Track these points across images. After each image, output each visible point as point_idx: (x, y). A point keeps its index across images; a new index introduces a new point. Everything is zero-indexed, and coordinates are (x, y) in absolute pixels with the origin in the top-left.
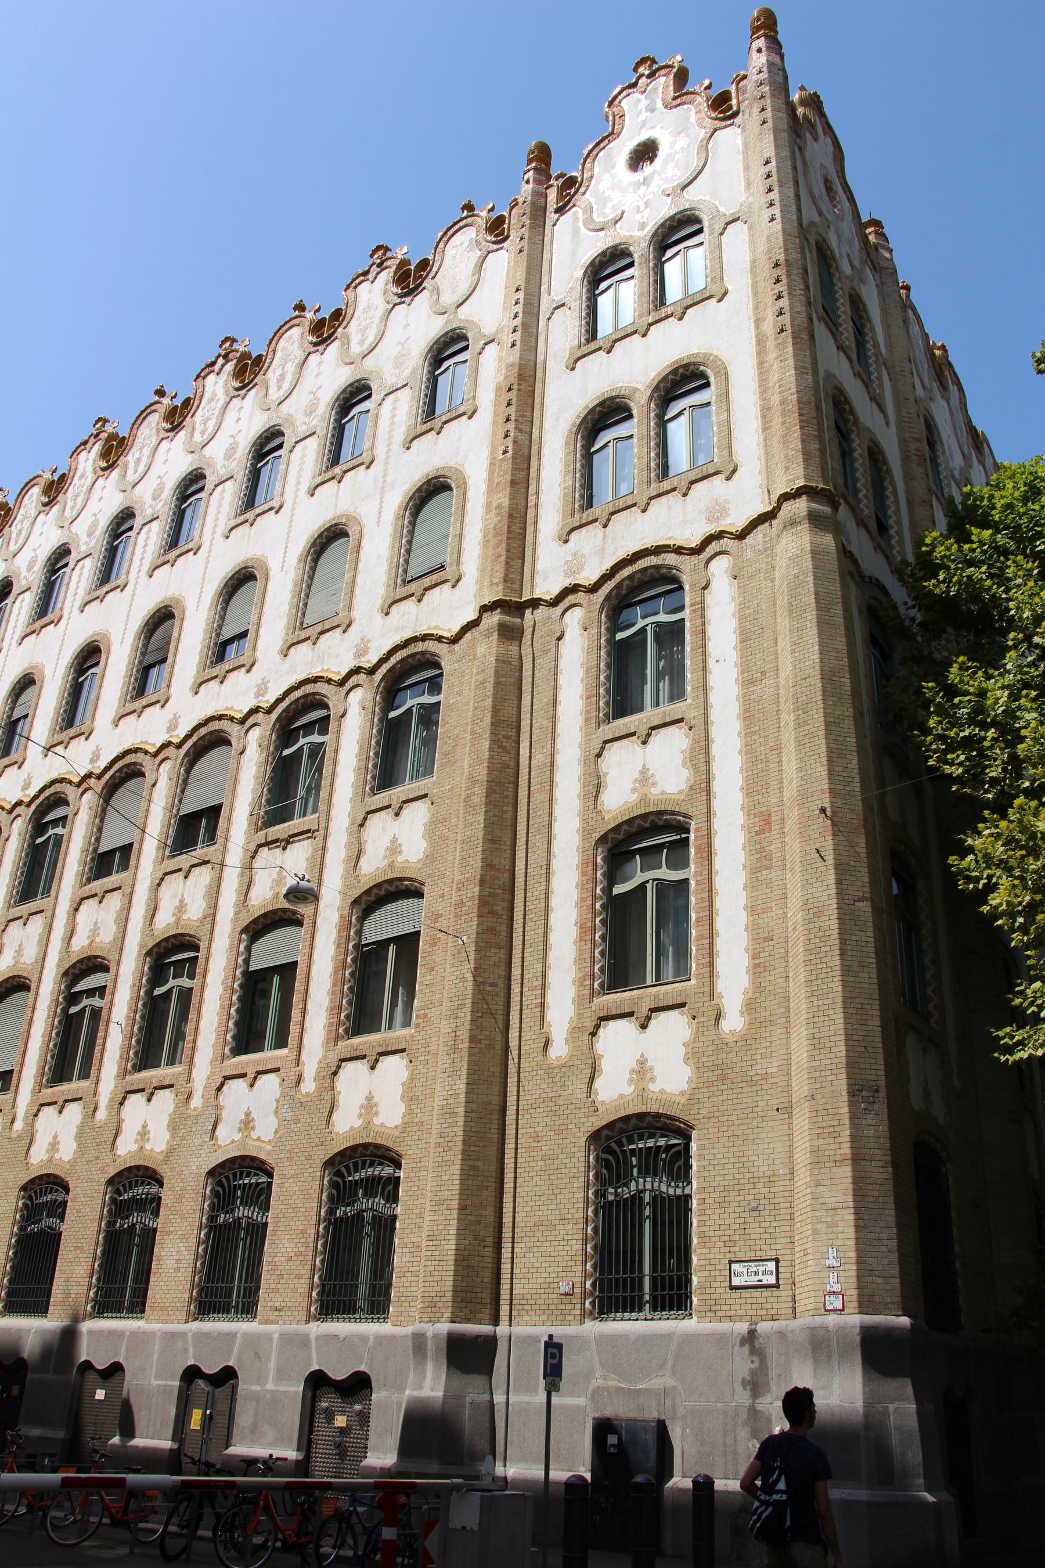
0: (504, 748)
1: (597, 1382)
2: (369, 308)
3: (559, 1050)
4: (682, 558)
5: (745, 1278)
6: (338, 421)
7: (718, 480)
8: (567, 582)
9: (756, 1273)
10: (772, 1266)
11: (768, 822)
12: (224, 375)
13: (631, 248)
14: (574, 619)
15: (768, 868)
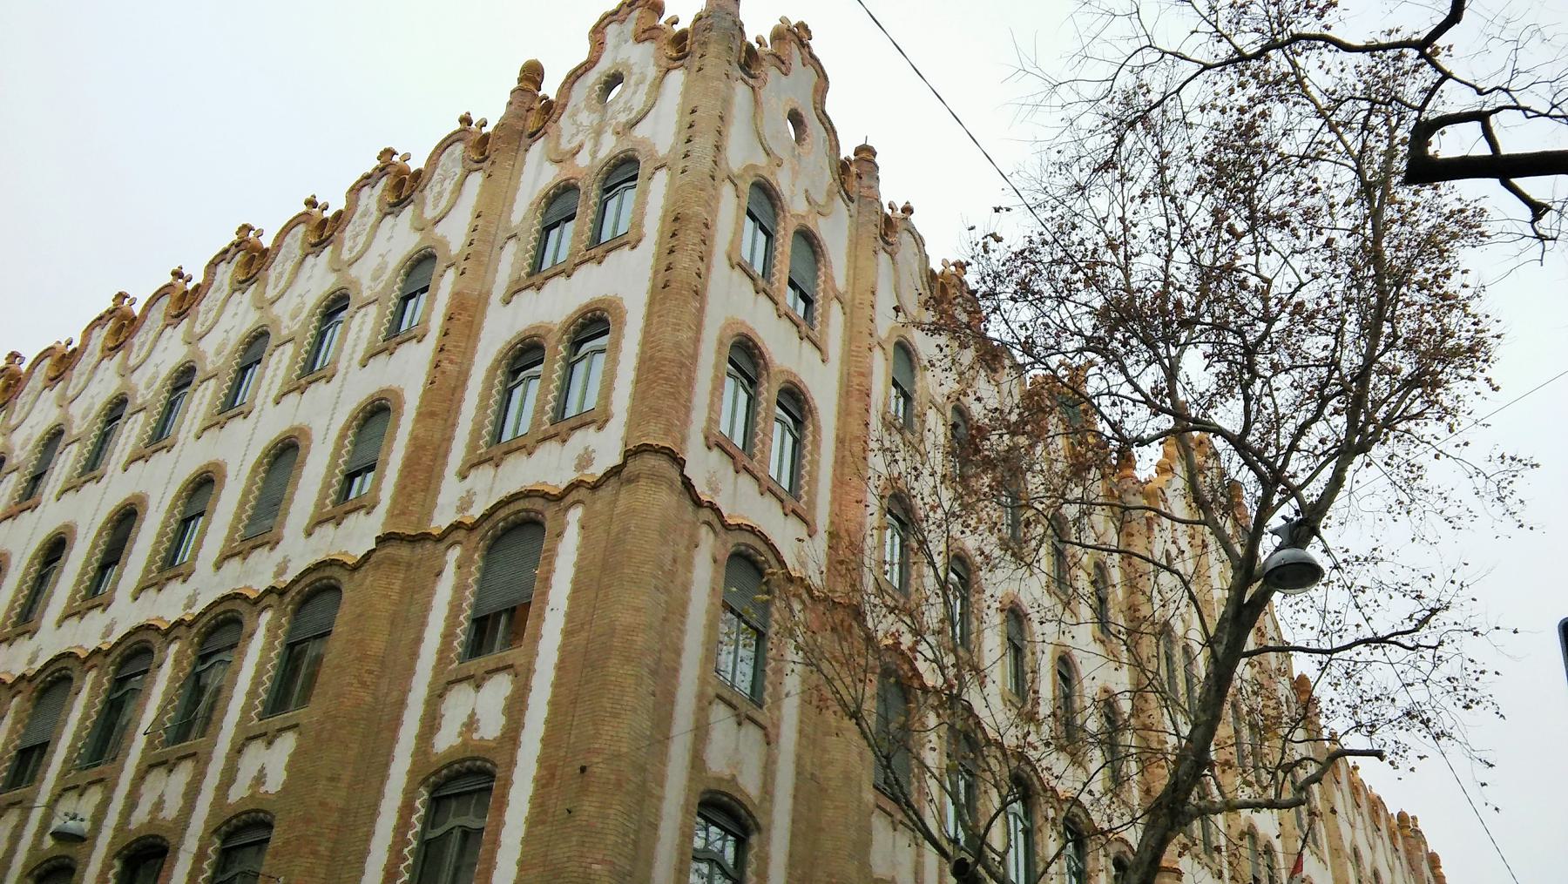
0: (364, 684)
2: (364, 215)
7: (592, 429)
8: (458, 518)
11: (553, 776)
12: (233, 265)
14: (454, 554)
15: (543, 822)
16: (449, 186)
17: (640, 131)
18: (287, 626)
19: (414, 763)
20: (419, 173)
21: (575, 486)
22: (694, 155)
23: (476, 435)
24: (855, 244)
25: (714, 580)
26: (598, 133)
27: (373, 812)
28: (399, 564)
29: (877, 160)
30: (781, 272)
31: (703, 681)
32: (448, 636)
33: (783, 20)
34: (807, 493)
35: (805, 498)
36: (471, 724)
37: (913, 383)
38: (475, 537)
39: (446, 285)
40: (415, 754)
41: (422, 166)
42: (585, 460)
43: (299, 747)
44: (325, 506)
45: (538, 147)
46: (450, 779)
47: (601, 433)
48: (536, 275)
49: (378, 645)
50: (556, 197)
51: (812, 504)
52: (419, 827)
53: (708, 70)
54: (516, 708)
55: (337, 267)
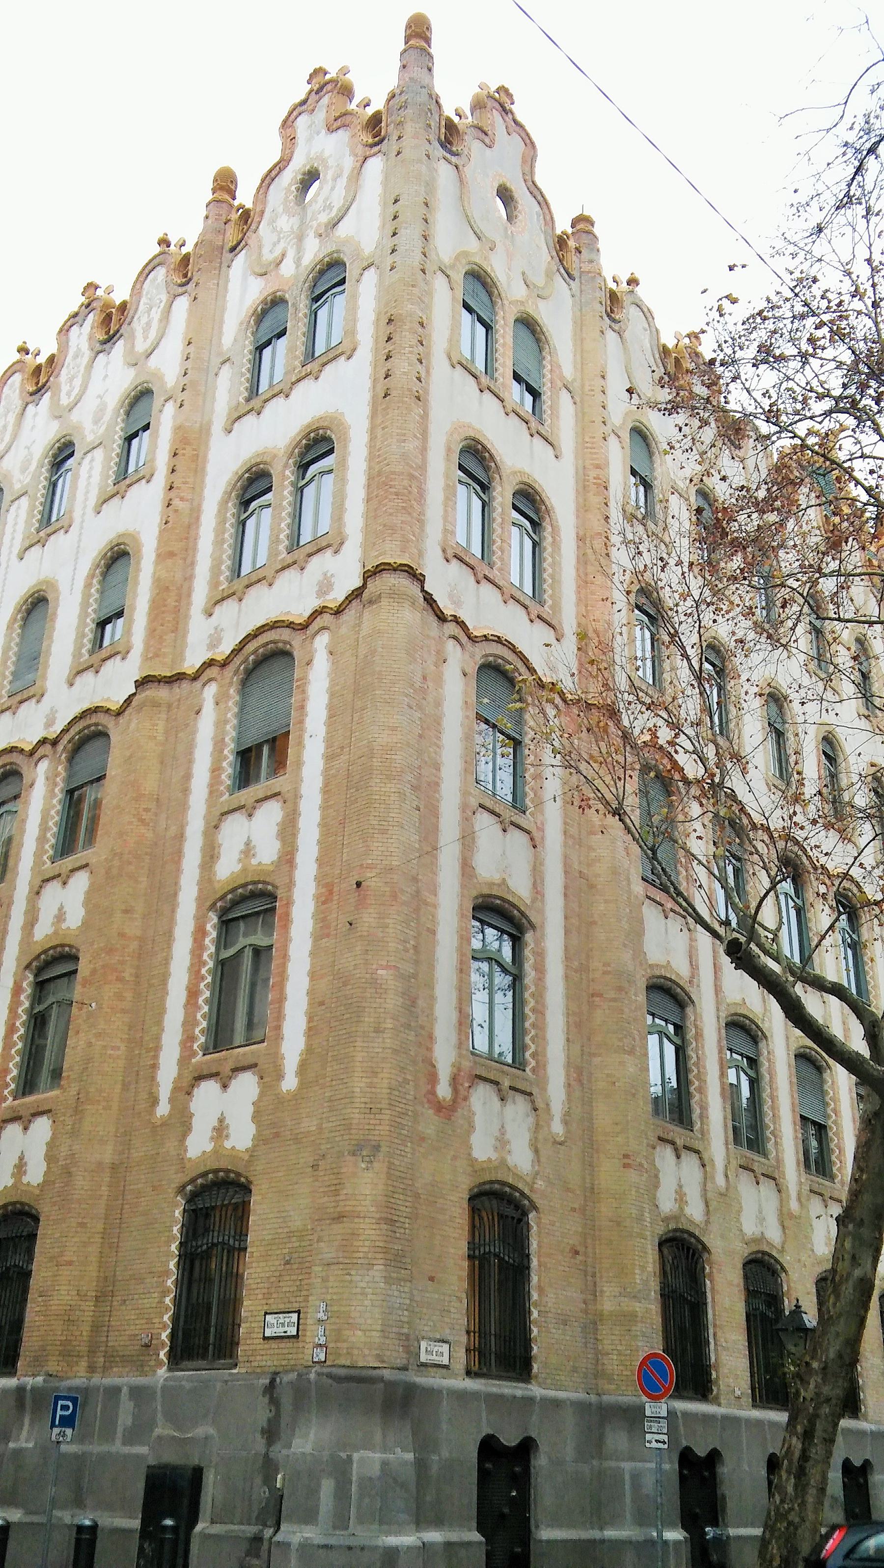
0: (142, 821)
1: (158, 1431)
3: (163, 1109)
4: (294, 634)
5: (275, 1329)
7: (329, 553)
9: (283, 1325)
10: (295, 1316)
11: (331, 892)
13: (287, 296)
14: (210, 691)
15: (328, 936)
16: (156, 314)
17: (343, 230)
18: (64, 774)
19: (200, 890)
20: (123, 307)
21: (317, 613)
22: (401, 249)
23: (215, 570)
24: (579, 325)
25: (466, 693)
26: (300, 238)
27: (169, 937)
28: (159, 705)
29: (596, 230)
30: (504, 365)
31: (465, 793)
32: (216, 770)
33: (139, 533)
34: (551, 597)
35: (549, 602)
36: (248, 850)
37: (652, 469)
38: (229, 670)
39: (166, 420)
40: (200, 883)
41: (127, 297)
42: (325, 586)
43: (92, 885)
44: (81, 655)
45: (240, 260)
46: (235, 903)
47: (338, 557)
48: (255, 397)
49: (150, 785)
50: (264, 312)
51: (556, 607)
52: (212, 949)
53: (407, 153)
54: (288, 832)
55: (58, 414)
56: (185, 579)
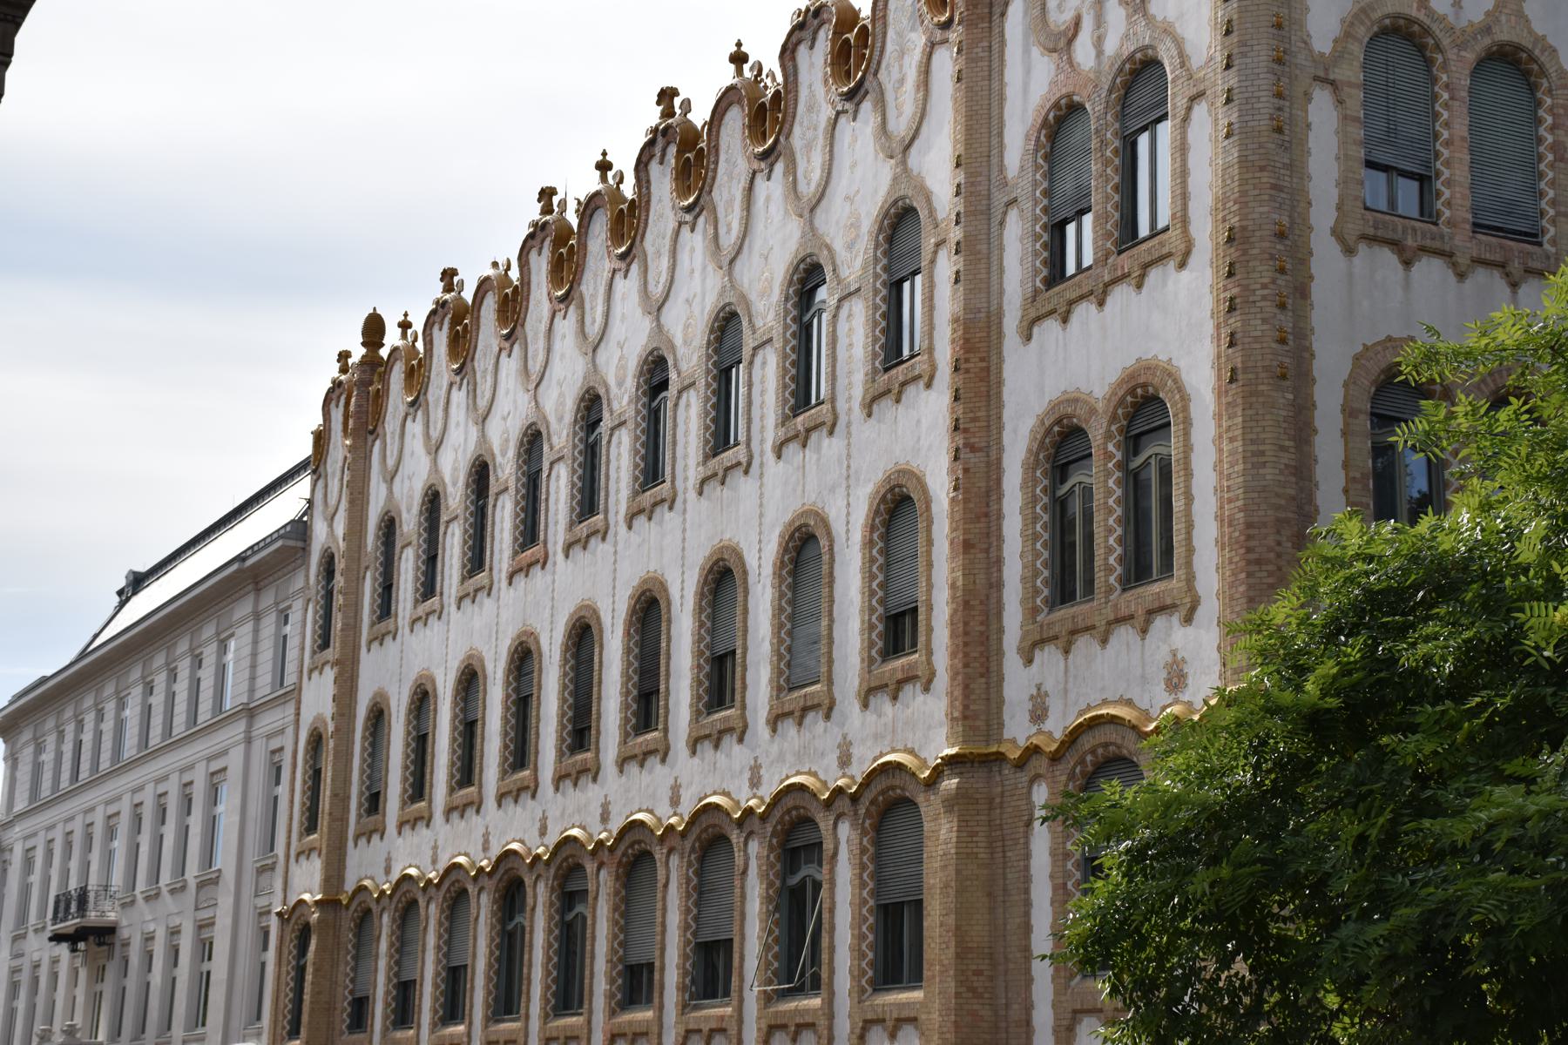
0: (972, 990)
6: (798, 320)
56: (991, 586)
